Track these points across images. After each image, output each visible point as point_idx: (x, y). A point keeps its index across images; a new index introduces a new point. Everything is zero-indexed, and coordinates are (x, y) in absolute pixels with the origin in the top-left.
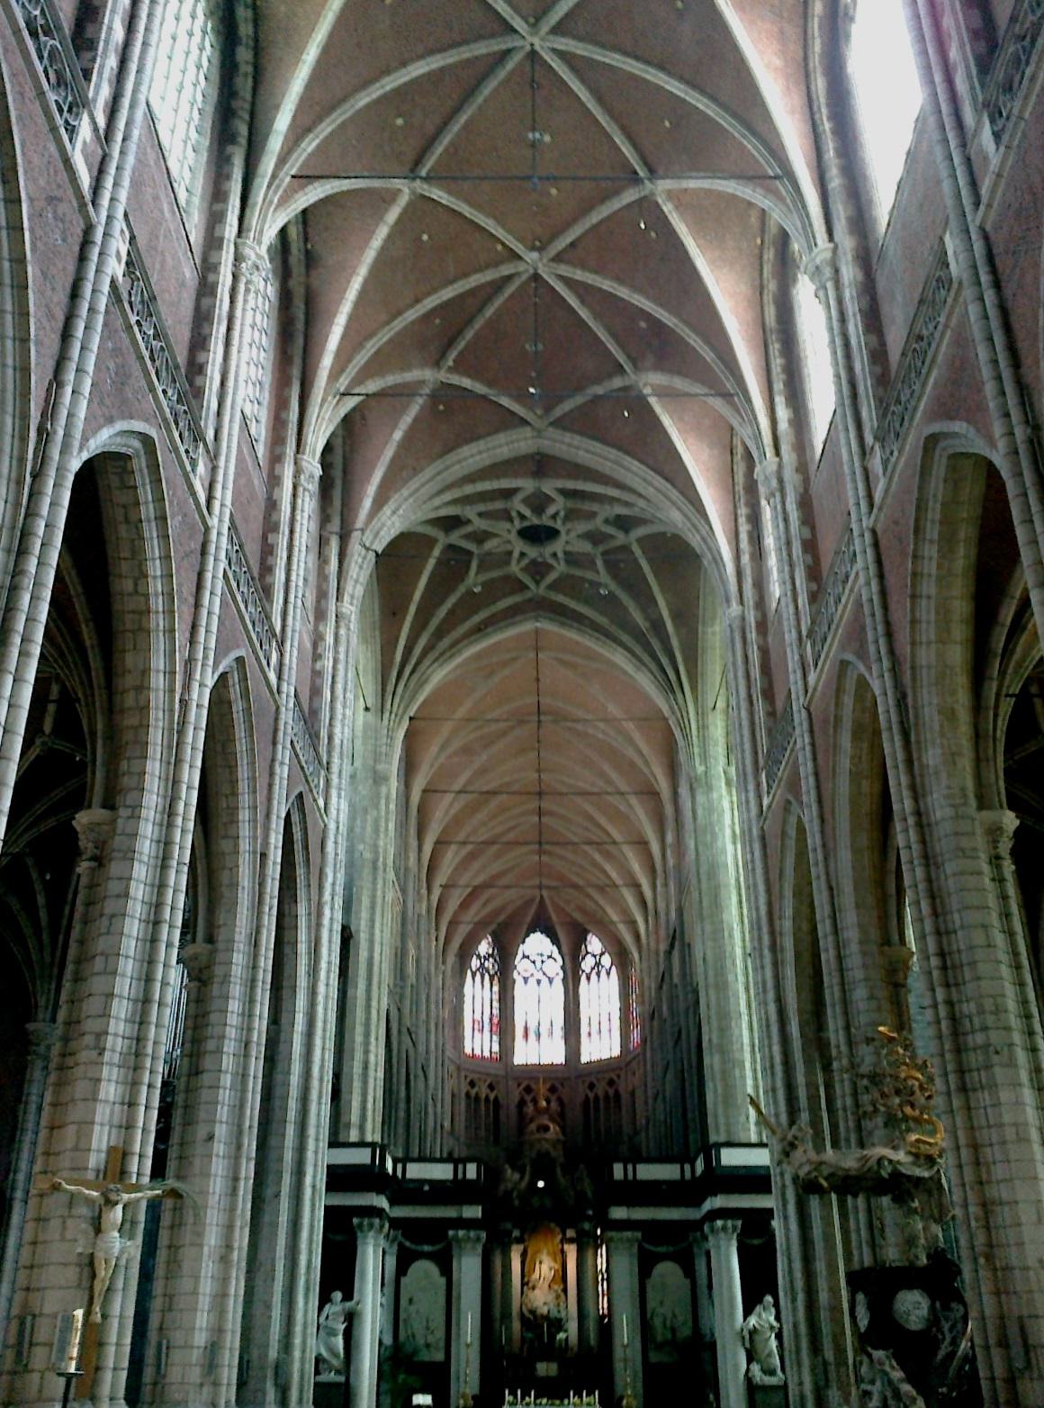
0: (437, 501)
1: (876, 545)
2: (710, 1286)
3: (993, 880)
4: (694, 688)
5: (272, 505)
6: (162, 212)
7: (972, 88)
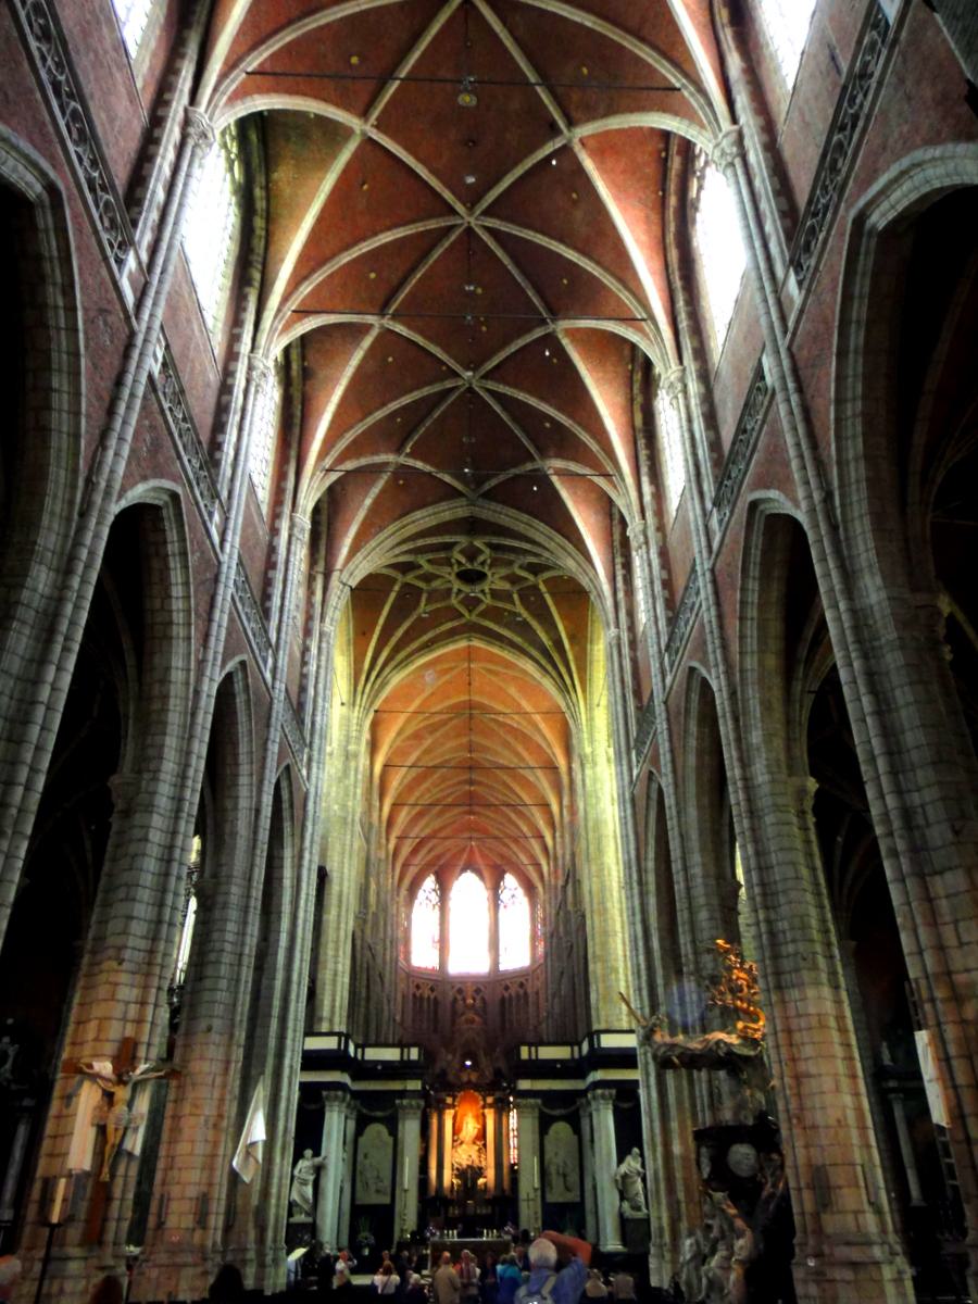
0: (397, 551)
1: (714, 582)
2: (592, 1141)
3: (800, 829)
4: (584, 691)
5: (272, 549)
6: (193, 331)
7: (782, 252)
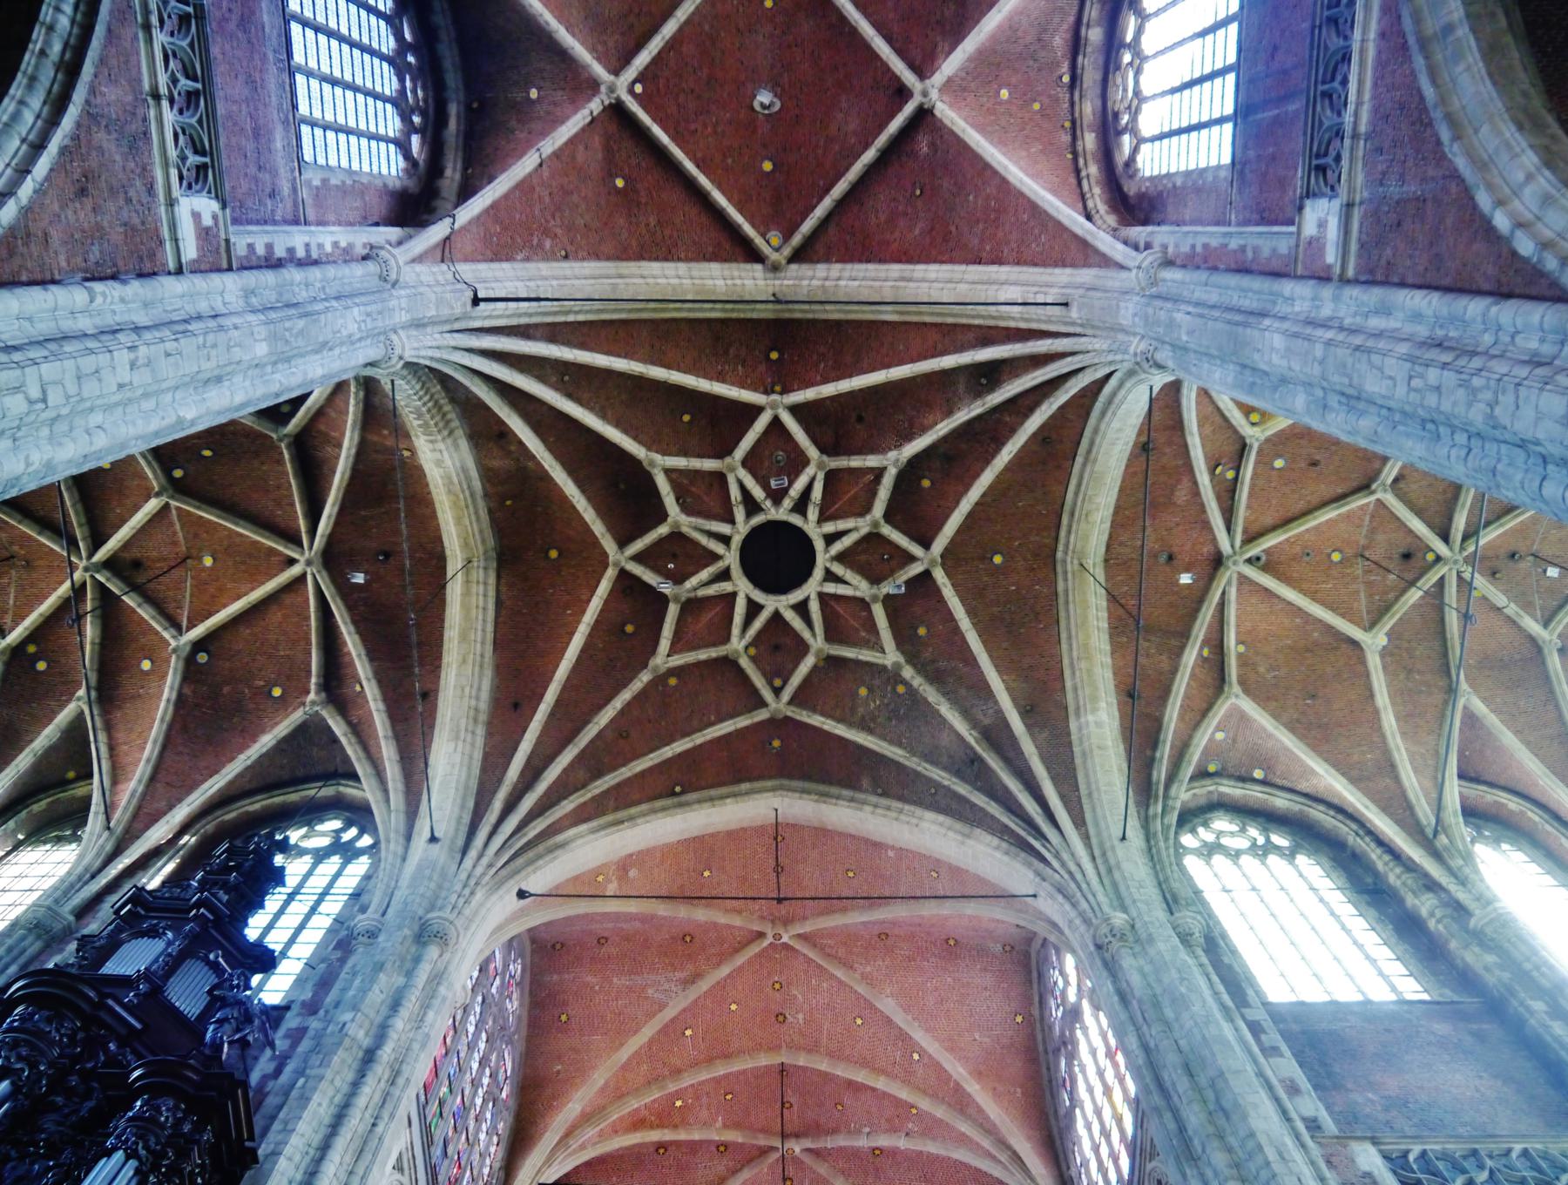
4: (1079, 822)
